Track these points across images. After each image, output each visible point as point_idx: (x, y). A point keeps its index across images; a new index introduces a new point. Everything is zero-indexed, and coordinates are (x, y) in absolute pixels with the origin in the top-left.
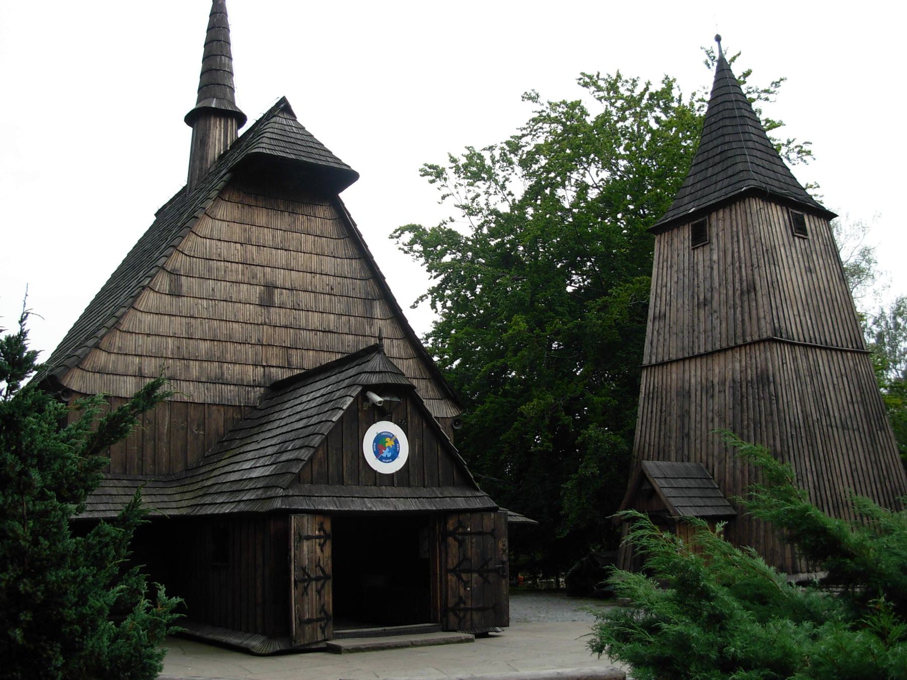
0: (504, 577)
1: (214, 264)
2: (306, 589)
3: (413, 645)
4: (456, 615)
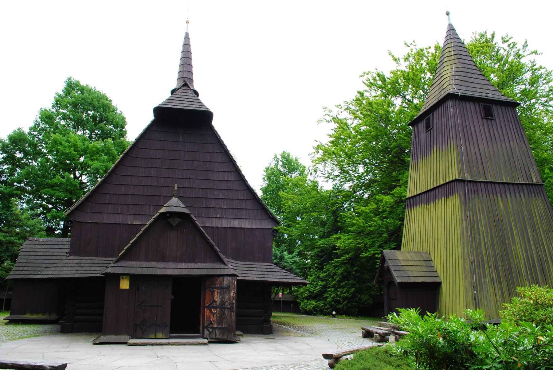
0: (233, 312)
3: (169, 344)
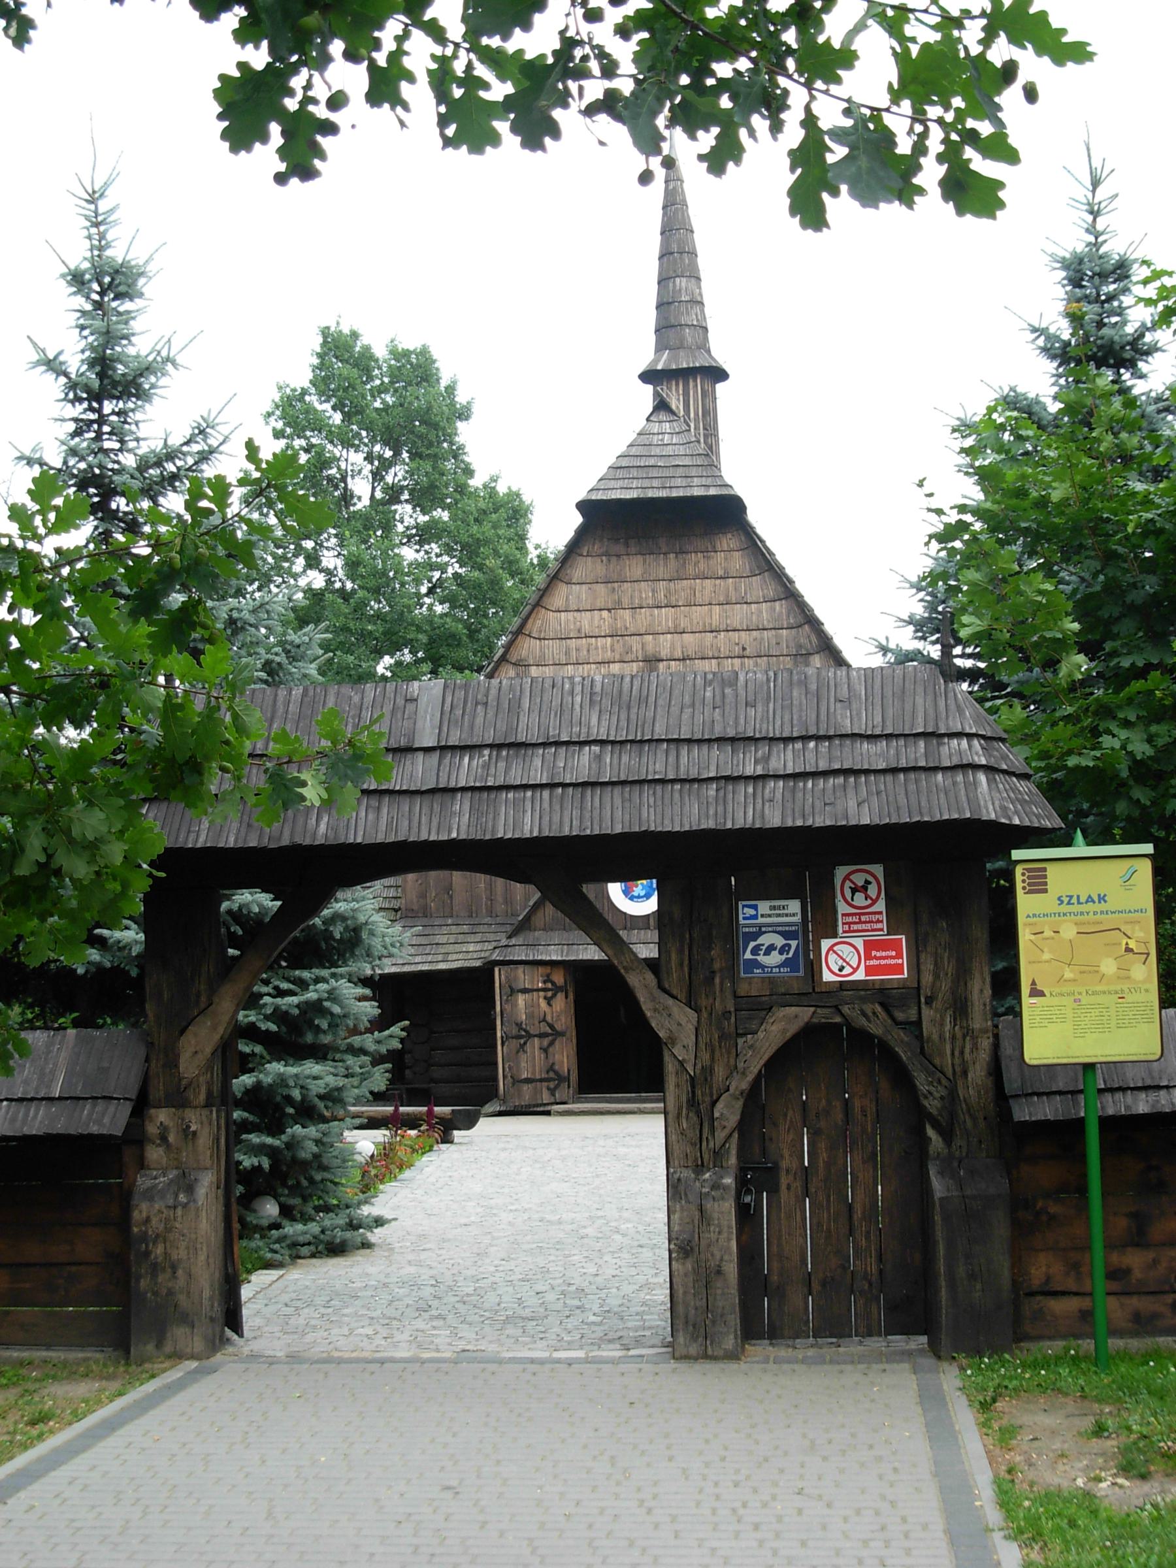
1: (573, 643)
2: (523, 1046)
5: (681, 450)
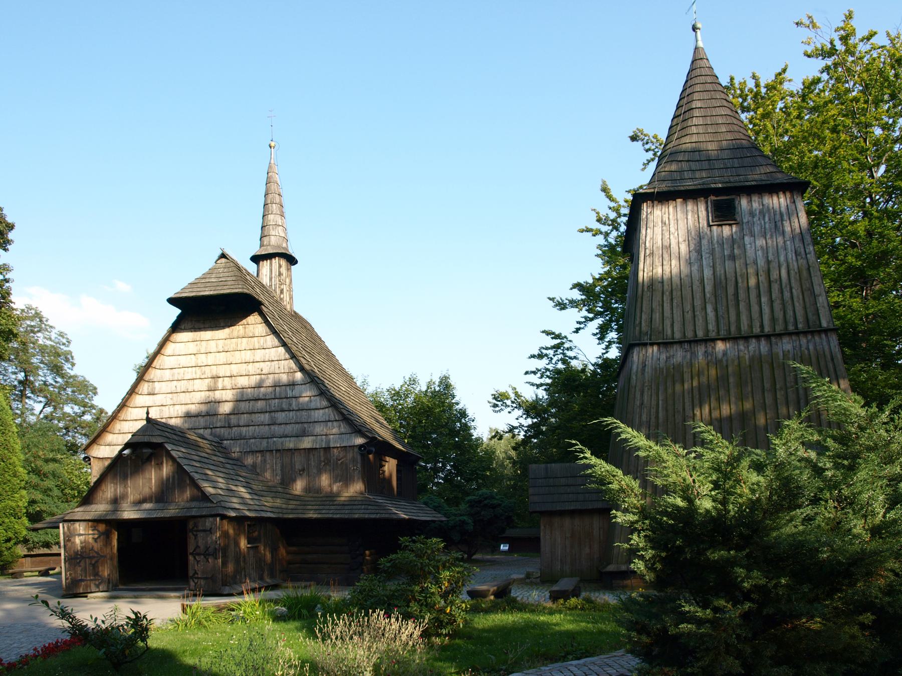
4: (193, 581)
5: (227, 274)
